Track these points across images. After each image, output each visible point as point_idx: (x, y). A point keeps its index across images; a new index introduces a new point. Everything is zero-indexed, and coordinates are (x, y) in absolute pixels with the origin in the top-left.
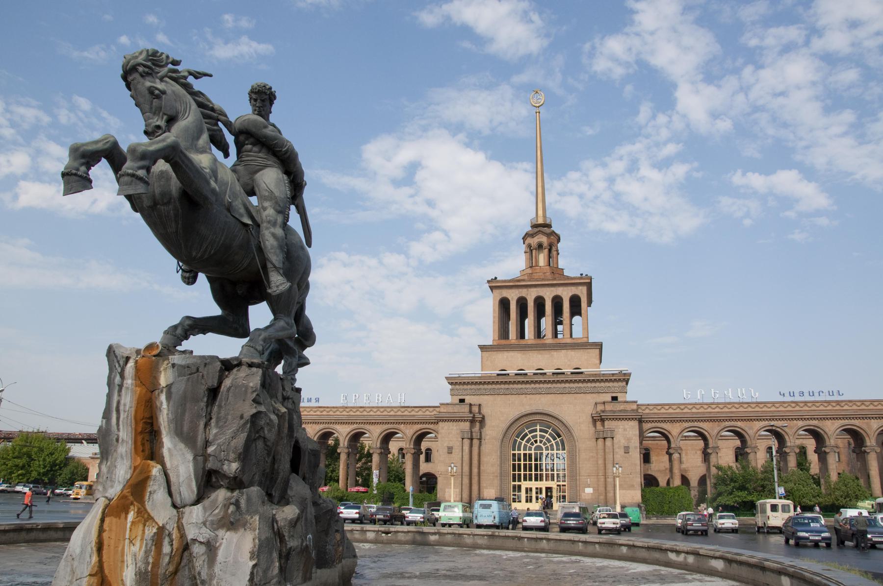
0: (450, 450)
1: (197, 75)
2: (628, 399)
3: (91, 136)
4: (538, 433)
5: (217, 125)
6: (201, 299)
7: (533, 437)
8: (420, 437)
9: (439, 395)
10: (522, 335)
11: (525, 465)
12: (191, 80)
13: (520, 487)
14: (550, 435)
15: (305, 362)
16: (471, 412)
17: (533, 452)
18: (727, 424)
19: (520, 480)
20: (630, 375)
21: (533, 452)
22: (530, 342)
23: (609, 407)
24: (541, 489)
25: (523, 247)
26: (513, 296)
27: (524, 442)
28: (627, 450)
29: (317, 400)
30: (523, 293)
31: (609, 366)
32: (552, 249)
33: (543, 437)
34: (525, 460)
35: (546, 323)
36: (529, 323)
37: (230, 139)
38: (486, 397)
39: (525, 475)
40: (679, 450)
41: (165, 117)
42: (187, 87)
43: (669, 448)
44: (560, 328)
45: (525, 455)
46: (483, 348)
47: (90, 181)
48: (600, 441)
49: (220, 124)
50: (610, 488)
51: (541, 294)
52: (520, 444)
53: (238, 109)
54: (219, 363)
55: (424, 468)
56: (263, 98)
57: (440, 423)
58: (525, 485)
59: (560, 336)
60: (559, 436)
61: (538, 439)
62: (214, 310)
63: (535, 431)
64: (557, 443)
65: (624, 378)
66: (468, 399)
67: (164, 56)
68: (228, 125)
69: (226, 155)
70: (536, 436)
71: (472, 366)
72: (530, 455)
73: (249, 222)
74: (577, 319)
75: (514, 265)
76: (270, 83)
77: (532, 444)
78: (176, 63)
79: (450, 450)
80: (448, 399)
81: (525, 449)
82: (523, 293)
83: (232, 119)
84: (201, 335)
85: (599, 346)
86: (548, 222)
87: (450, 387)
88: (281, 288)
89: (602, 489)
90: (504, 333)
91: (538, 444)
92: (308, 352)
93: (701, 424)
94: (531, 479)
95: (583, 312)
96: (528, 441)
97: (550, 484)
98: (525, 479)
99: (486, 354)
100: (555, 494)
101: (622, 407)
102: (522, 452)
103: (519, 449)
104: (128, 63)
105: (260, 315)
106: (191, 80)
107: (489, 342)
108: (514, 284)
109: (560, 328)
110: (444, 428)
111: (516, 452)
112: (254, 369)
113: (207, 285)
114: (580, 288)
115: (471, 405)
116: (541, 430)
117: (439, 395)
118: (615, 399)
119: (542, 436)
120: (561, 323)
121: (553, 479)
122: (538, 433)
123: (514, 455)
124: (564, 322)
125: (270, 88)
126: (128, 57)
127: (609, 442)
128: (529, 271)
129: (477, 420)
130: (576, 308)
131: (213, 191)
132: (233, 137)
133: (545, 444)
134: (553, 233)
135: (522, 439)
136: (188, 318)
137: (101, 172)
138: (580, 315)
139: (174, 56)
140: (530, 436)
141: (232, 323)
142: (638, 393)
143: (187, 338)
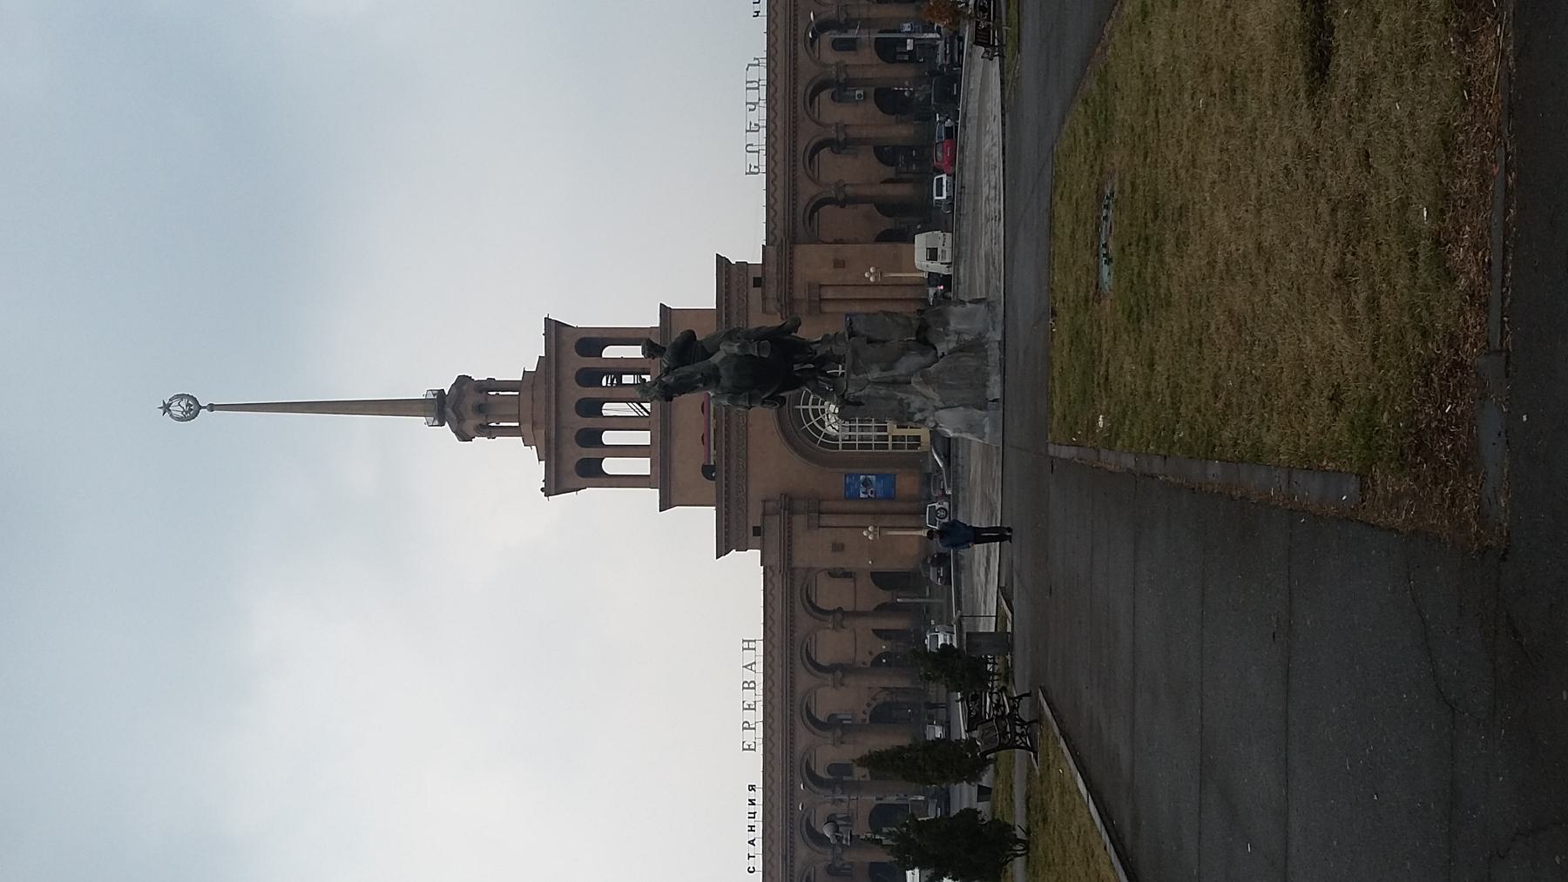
0: (838, 547)
4: (810, 407)
13: (895, 438)
18: (800, 109)
23: (772, 290)
25: (479, 441)
28: (839, 264)
29: (752, 788)
30: (569, 435)
31: (701, 295)
38: (750, 492)
40: (840, 186)
46: (665, 505)
48: (828, 308)
50: (897, 293)
57: (797, 563)
66: (755, 521)
79: (838, 547)
80: (754, 555)
82: (569, 435)
93: (801, 147)
98: (885, 429)
101: (772, 269)
108: (551, 455)
110: (802, 558)
115: (764, 514)
118: (758, 282)
122: (810, 407)
127: (829, 294)
128: (527, 428)
129: (788, 504)
142: (749, 247)
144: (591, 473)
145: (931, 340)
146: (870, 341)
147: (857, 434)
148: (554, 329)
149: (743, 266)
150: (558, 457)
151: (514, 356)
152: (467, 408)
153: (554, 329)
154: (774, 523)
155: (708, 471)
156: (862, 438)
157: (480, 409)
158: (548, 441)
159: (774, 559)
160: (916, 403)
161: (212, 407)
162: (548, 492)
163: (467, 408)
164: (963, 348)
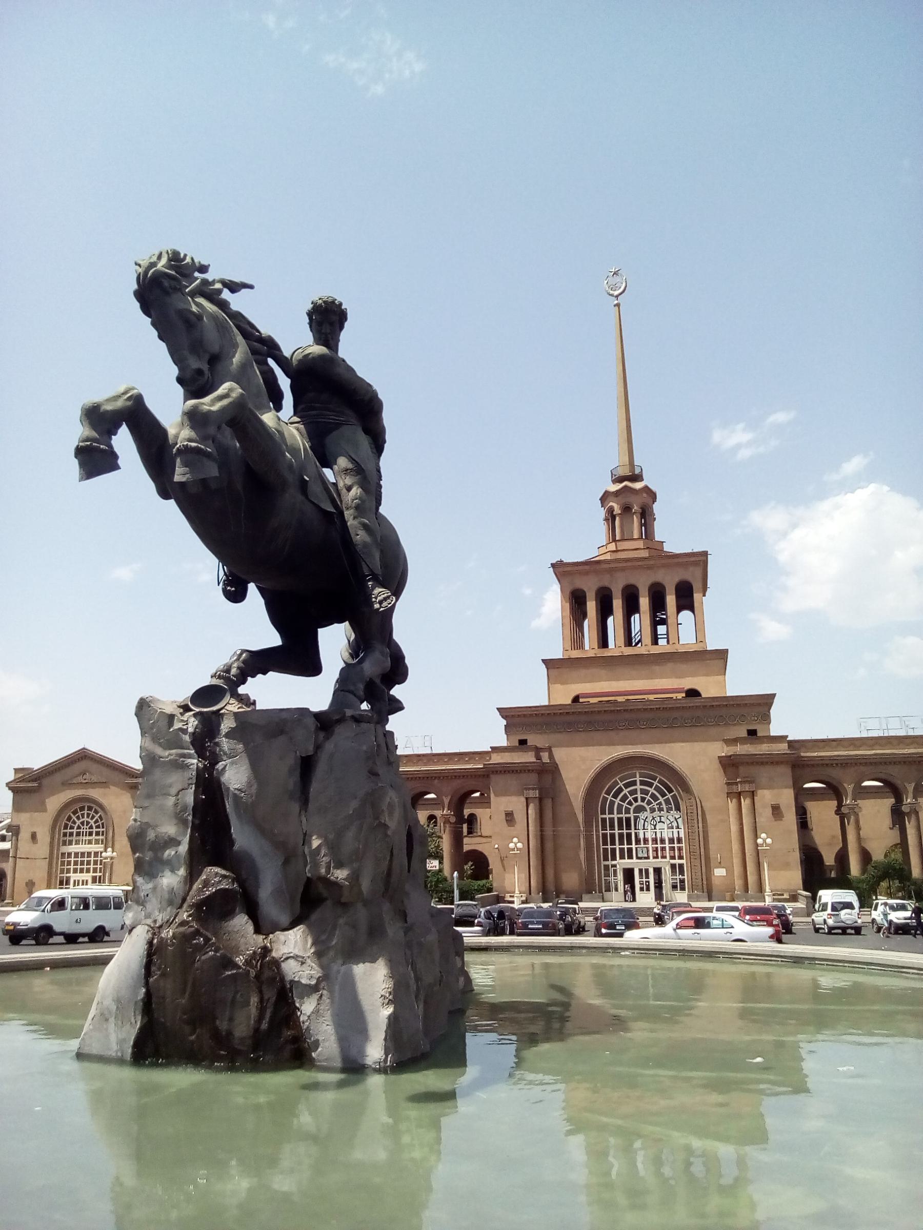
0: (510, 817)
1: (234, 287)
2: (773, 733)
3: (106, 390)
4: (638, 787)
5: (267, 364)
6: (253, 624)
7: (631, 793)
8: (461, 800)
9: (490, 735)
10: (604, 643)
11: (621, 835)
12: (226, 295)
14: (657, 789)
15: (396, 706)
16: (538, 757)
17: (632, 815)
19: (614, 858)
20: (774, 695)
21: (632, 815)
22: (617, 653)
24: (647, 871)
25: (602, 513)
26: (590, 587)
27: (617, 801)
28: (776, 810)
31: (738, 682)
32: (646, 515)
33: (646, 793)
34: (621, 827)
35: (640, 622)
36: (614, 624)
37: (284, 383)
39: (622, 850)
41: (207, 357)
42: (223, 305)
43: (840, 806)
44: (661, 629)
45: (620, 820)
47: (115, 456)
49: (271, 362)
51: (632, 581)
52: (612, 803)
53: (296, 339)
54: (313, 719)
55: (469, 844)
56: (327, 319)
58: (622, 863)
59: (663, 642)
60: (670, 791)
61: (639, 795)
62: (271, 638)
63: (634, 783)
64: (667, 802)
65: (762, 705)
66: (534, 740)
67: (188, 260)
68: (283, 362)
69: (278, 407)
70: (635, 792)
71: (535, 692)
72: (628, 820)
73: (333, 510)
74: (686, 615)
75: (589, 540)
76: (339, 298)
77: (630, 803)
78: (203, 269)
80: (502, 740)
81: (619, 812)
83: (287, 353)
84: (260, 676)
85: (722, 655)
86: (637, 471)
87: (504, 722)
88: (385, 604)
89: (737, 869)
90: (577, 641)
91: (639, 803)
92: (397, 691)
94: (630, 857)
95: (696, 605)
96: (623, 800)
97: (659, 862)
98: (622, 857)
99: (554, 672)
100: (667, 877)
102: (615, 816)
103: (611, 812)
104: (146, 272)
105: (334, 641)
106: (226, 295)
107: (559, 655)
109: (661, 629)
111: (607, 816)
112: (364, 726)
113: (262, 601)
114: (691, 569)
116: (642, 783)
117: (490, 735)
118: (752, 733)
119: (644, 792)
120: (663, 622)
121: (664, 857)
122: (638, 787)
123: (604, 820)
124: (669, 621)
125: (341, 304)
126: (145, 263)
128: (612, 547)
130: (686, 600)
131: (290, 466)
132: (288, 381)
133: (649, 803)
134: (647, 489)
135: (615, 796)
136: (243, 651)
137: (124, 442)
138: (692, 610)
139: (200, 259)
140: (626, 791)
141: (298, 657)
143: (244, 682)
144: (576, 602)
145: (314, 917)
146: (307, 766)
147: (617, 832)
148: (700, 560)
149: (766, 718)
150: (587, 573)
151: (674, 533)
152: (630, 503)
153: (699, 560)
154: (528, 757)
155: (576, 699)
156: (613, 836)
157: (627, 509)
158: (598, 562)
159: (496, 759)
160: (171, 880)
161: (618, 305)
162: (553, 565)
163: (630, 503)
164: (282, 996)
